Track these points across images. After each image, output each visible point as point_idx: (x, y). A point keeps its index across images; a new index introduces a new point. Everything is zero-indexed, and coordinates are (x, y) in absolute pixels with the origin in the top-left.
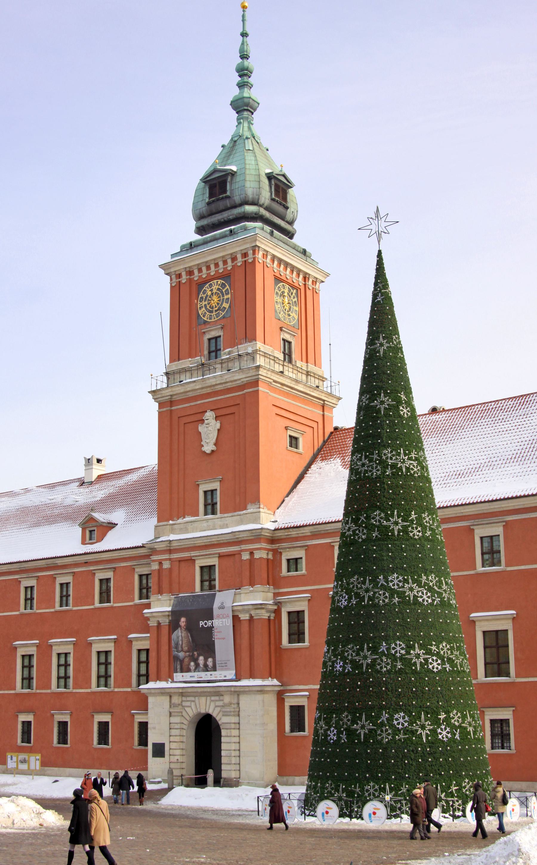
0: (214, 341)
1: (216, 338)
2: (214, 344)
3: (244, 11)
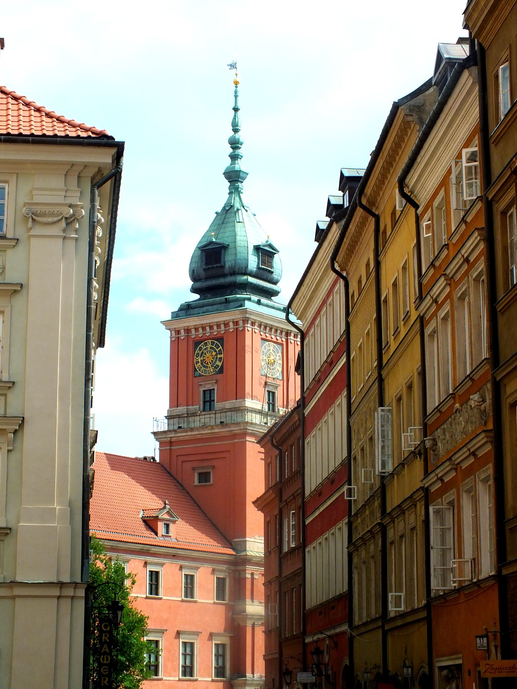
0: (208, 392)
1: (210, 390)
2: (208, 396)
3: (236, 87)
